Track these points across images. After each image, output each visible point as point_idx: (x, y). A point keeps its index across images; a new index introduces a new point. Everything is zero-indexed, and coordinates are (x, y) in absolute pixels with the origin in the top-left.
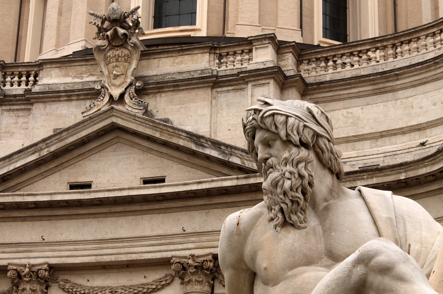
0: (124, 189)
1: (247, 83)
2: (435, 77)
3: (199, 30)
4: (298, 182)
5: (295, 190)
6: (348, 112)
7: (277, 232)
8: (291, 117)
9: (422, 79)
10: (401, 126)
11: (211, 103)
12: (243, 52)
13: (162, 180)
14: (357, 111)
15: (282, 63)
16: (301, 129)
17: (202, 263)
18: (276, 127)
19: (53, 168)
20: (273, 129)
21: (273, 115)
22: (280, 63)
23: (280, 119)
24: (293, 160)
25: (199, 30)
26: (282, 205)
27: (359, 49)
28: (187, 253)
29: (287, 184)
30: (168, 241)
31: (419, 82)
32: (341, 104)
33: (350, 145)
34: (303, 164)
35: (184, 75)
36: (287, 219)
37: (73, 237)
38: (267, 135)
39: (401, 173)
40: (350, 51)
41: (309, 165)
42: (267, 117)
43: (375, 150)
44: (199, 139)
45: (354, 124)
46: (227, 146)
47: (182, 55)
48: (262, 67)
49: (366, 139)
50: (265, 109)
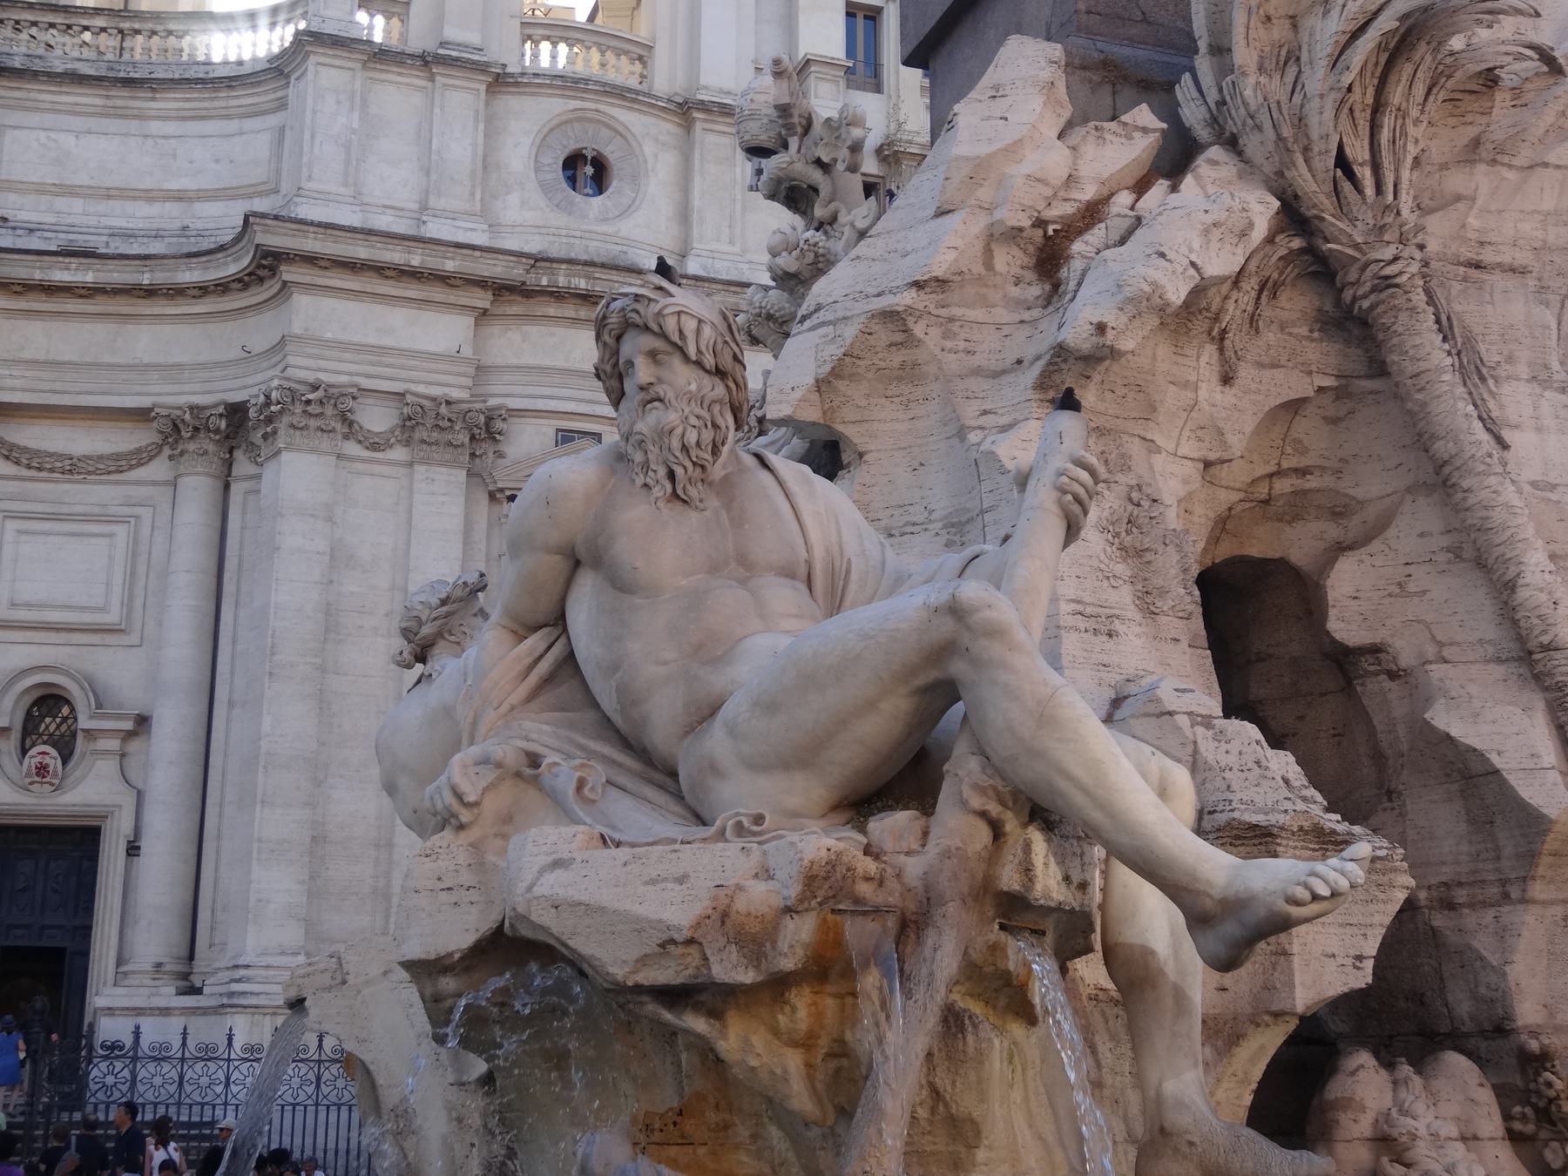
6: (48, 137)
20: (676, 338)
21: (679, 313)
23: (690, 325)
26: (675, 467)
27: (85, 22)
29: (692, 437)
32: (35, 119)
33: (45, 198)
38: (659, 344)
49: (77, 195)
50: (664, 301)
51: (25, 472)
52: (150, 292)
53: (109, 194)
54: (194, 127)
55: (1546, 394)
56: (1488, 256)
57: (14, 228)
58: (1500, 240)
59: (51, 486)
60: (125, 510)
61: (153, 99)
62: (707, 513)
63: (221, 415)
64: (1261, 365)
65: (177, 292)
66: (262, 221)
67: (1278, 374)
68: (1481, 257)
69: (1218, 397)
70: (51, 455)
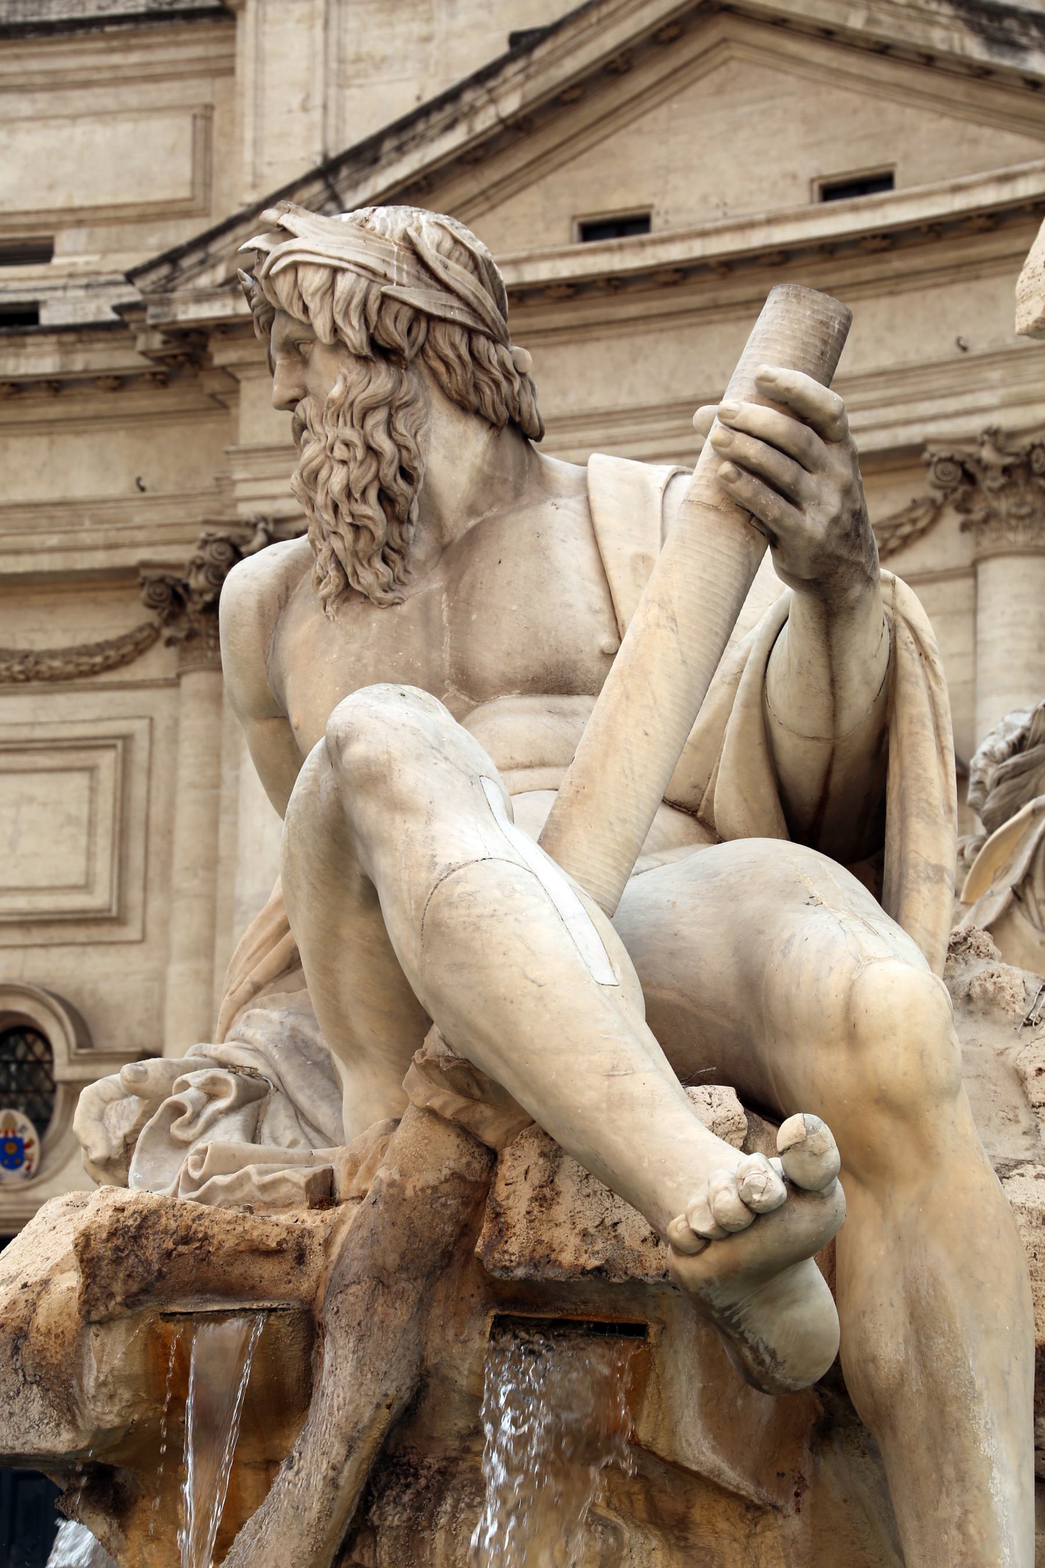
0: (751, 225)
4: (362, 475)
5: (357, 496)
7: (328, 617)
8: (344, 270)
13: (882, 181)
16: (373, 306)
17: (1029, 454)
18: (306, 309)
19: (519, 170)
21: (295, 266)
24: (352, 404)
28: (975, 424)
29: (337, 479)
30: (909, 390)
34: (381, 415)
36: (350, 580)
37: (600, 399)
41: (401, 414)
42: (278, 274)
44: (1000, 21)
62: (403, 609)
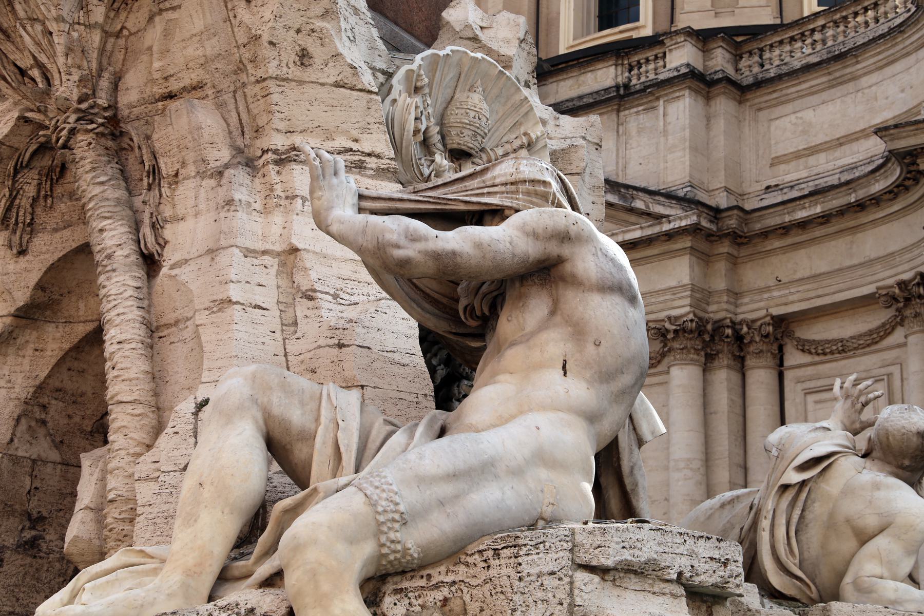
1: (658, 99)
2: (904, 51)
3: (644, 27)
6: (797, 118)
9: (889, 56)
10: (863, 127)
11: (618, 132)
12: (656, 58)
14: (808, 115)
15: (710, 63)
22: (707, 63)
25: (644, 27)
27: (811, 26)
31: (885, 62)
32: (789, 107)
33: (802, 161)
35: (585, 100)
39: (850, 194)
40: (800, 31)
43: (830, 166)
45: (804, 132)
46: (627, 187)
47: (584, 73)
48: (676, 74)
51: (817, 359)
52: (860, 206)
53: (841, 142)
54: (889, 71)
55: (204, 183)
56: (174, 86)
57: (782, 189)
58: (176, 70)
59: (834, 365)
60: (884, 371)
61: (858, 62)
63: (918, 284)
64: (56, 230)
65: (876, 201)
66: (887, 133)
67: (66, 233)
68: (169, 89)
69: (11, 267)
70: (828, 342)
